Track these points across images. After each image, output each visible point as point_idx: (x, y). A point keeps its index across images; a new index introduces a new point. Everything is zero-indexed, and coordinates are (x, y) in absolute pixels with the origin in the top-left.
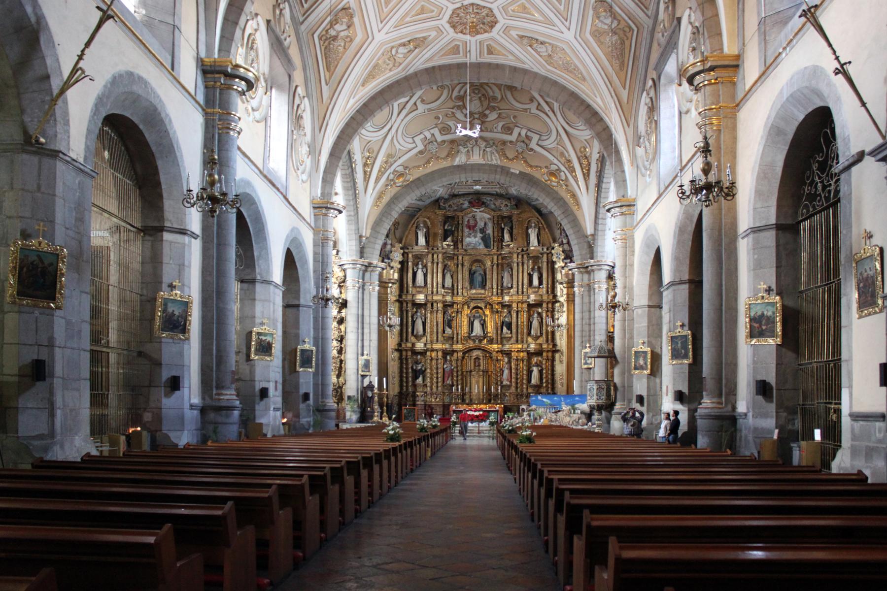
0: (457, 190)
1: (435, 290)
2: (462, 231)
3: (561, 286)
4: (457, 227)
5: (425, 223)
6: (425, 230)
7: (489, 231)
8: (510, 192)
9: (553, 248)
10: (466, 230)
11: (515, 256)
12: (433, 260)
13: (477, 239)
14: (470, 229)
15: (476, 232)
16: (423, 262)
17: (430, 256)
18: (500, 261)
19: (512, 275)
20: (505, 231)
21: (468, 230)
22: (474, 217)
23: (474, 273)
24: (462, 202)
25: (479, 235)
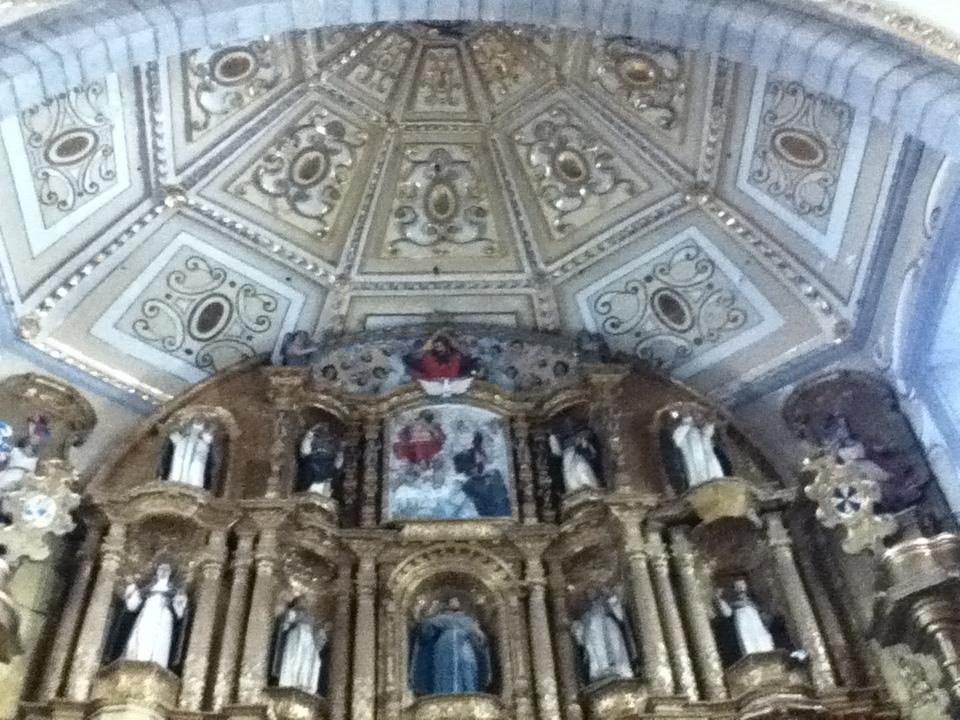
0: (361, 309)
1: (222, 688)
2: (381, 468)
3: (901, 649)
6: (208, 438)
8: (574, 325)
9: (808, 477)
10: (396, 464)
11: (633, 531)
13: (445, 492)
15: (439, 466)
17: (218, 540)
18: (558, 577)
19: (630, 630)
22: (428, 417)
24: (379, 359)
25: (454, 478)
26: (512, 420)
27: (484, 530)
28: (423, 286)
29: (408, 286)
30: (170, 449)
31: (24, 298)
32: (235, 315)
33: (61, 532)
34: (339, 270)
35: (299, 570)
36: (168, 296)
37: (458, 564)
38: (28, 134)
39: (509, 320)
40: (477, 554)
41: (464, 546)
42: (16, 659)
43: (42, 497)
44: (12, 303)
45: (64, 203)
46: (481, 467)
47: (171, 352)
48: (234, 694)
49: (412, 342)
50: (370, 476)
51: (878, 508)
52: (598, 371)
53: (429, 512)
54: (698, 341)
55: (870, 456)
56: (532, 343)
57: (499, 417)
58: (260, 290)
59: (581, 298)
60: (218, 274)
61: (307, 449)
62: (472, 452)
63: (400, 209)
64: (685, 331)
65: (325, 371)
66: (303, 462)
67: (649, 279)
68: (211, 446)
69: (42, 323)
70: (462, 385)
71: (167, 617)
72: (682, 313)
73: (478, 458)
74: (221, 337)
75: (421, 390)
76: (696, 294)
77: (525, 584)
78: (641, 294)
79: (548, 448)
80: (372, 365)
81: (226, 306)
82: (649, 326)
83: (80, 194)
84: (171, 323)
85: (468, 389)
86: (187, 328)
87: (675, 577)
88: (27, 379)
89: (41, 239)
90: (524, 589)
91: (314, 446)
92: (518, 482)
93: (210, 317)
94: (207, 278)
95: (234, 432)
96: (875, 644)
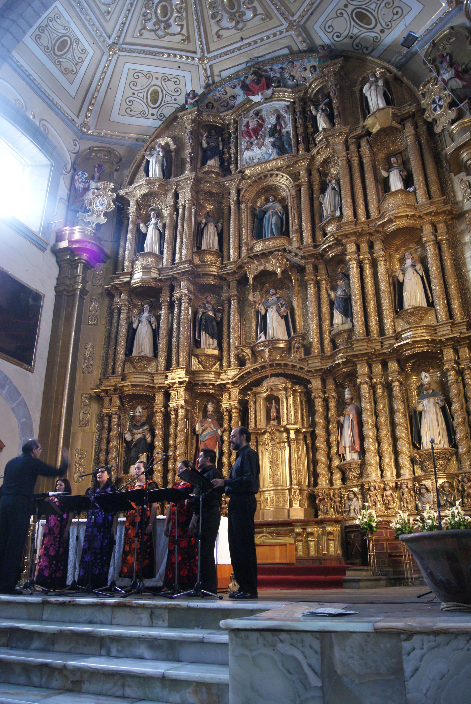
1: (177, 256)
4: (226, 143)
5: (166, 148)
7: (289, 128)
8: (318, 42)
10: (244, 143)
11: (340, 147)
12: (176, 203)
13: (263, 148)
14: (250, 137)
16: (159, 215)
20: (318, 117)
21: (247, 138)
22: (257, 114)
23: (265, 212)
24: (230, 92)
25: (268, 140)
26: (294, 103)
27: (280, 163)
28: (240, 48)
29: (233, 51)
30: (148, 162)
31: (78, 116)
32: (164, 92)
33: (109, 210)
34: (199, 55)
35: (209, 200)
36: (134, 94)
37: (270, 182)
38: (43, 48)
39: (286, 51)
40: (277, 175)
41: (271, 172)
42: (109, 261)
43: (101, 198)
44: (73, 120)
45: (73, 71)
46: (280, 131)
47: (145, 117)
48: (181, 258)
49: (242, 79)
50: (233, 151)
51: (452, 105)
52: (327, 66)
53: (256, 161)
54: (382, 31)
55: (458, 75)
56: (298, 61)
57: (288, 104)
58: (170, 77)
59: (317, 27)
60: (148, 76)
61: (205, 145)
62: (275, 126)
63: (213, 14)
64: (373, 28)
65: (207, 106)
66: (204, 151)
67: (346, 6)
68: (163, 157)
69: (90, 124)
70: (269, 92)
71: (157, 232)
72: (370, 19)
73: (278, 128)
74: (163, 104)
75: (251, 101)
76: (373, 6)
77: (297, 183)
78: (345, 15)
79: (311, 112)
80: (227, 96)
81: (159, 90)
82: (355, 31)
83: (77, 64)
84: (139, 106)
85: (273, 94)
86: (147, 105)
87: (361, 164)
88: (91, 149)
89: (72, 90)
90: (296, 185)
91: (208, 143)
92: (297, 135)
93: (155, 97)
94: (145, 80)
95: (173, 147)
96: (452, 174)
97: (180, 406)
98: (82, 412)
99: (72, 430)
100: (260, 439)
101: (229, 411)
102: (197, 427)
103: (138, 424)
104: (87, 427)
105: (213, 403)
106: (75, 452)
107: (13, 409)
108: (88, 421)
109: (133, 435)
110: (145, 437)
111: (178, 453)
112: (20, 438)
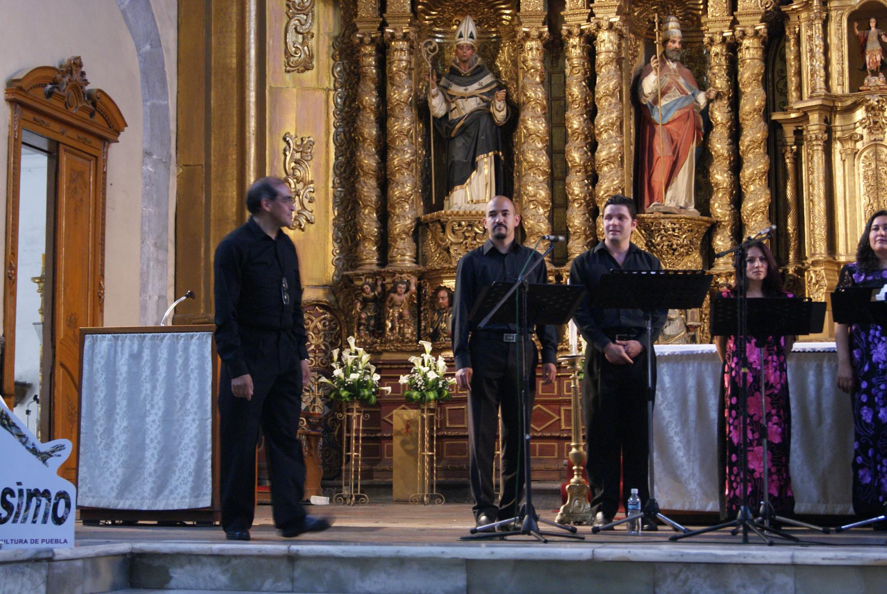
97: (605, 24)
98: (291, 29)
99: (269, 82)
100: (838, 121)
101: (733, 47)
102: (649, 84)
103: (465, 70)
104: (308, 73)
105: (674, 14)
106: (284, 145)
107: (124, 13)
108: (311, 57)
109: (449, 99)
110: (489, 104)
111: (602, 154)
112: (145, 101)
